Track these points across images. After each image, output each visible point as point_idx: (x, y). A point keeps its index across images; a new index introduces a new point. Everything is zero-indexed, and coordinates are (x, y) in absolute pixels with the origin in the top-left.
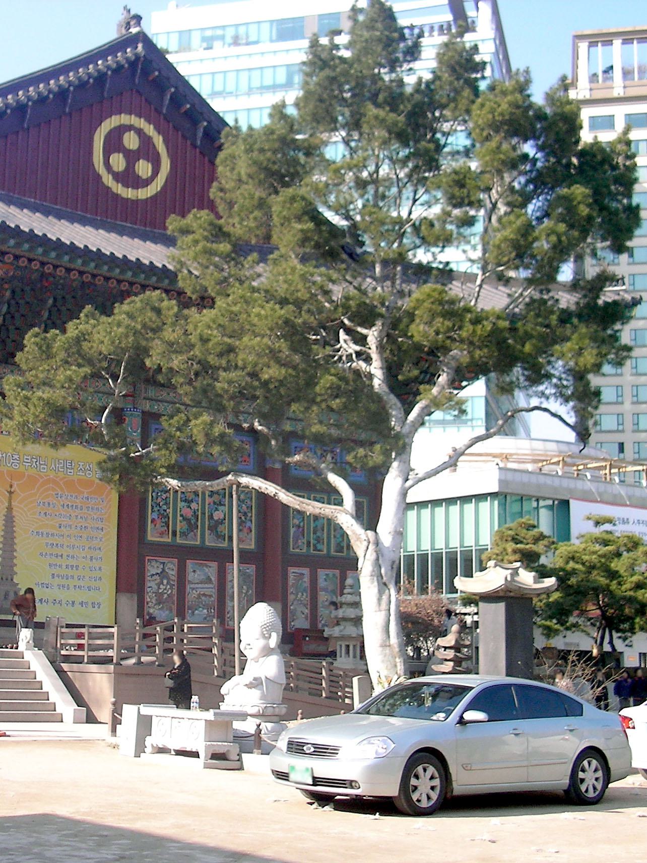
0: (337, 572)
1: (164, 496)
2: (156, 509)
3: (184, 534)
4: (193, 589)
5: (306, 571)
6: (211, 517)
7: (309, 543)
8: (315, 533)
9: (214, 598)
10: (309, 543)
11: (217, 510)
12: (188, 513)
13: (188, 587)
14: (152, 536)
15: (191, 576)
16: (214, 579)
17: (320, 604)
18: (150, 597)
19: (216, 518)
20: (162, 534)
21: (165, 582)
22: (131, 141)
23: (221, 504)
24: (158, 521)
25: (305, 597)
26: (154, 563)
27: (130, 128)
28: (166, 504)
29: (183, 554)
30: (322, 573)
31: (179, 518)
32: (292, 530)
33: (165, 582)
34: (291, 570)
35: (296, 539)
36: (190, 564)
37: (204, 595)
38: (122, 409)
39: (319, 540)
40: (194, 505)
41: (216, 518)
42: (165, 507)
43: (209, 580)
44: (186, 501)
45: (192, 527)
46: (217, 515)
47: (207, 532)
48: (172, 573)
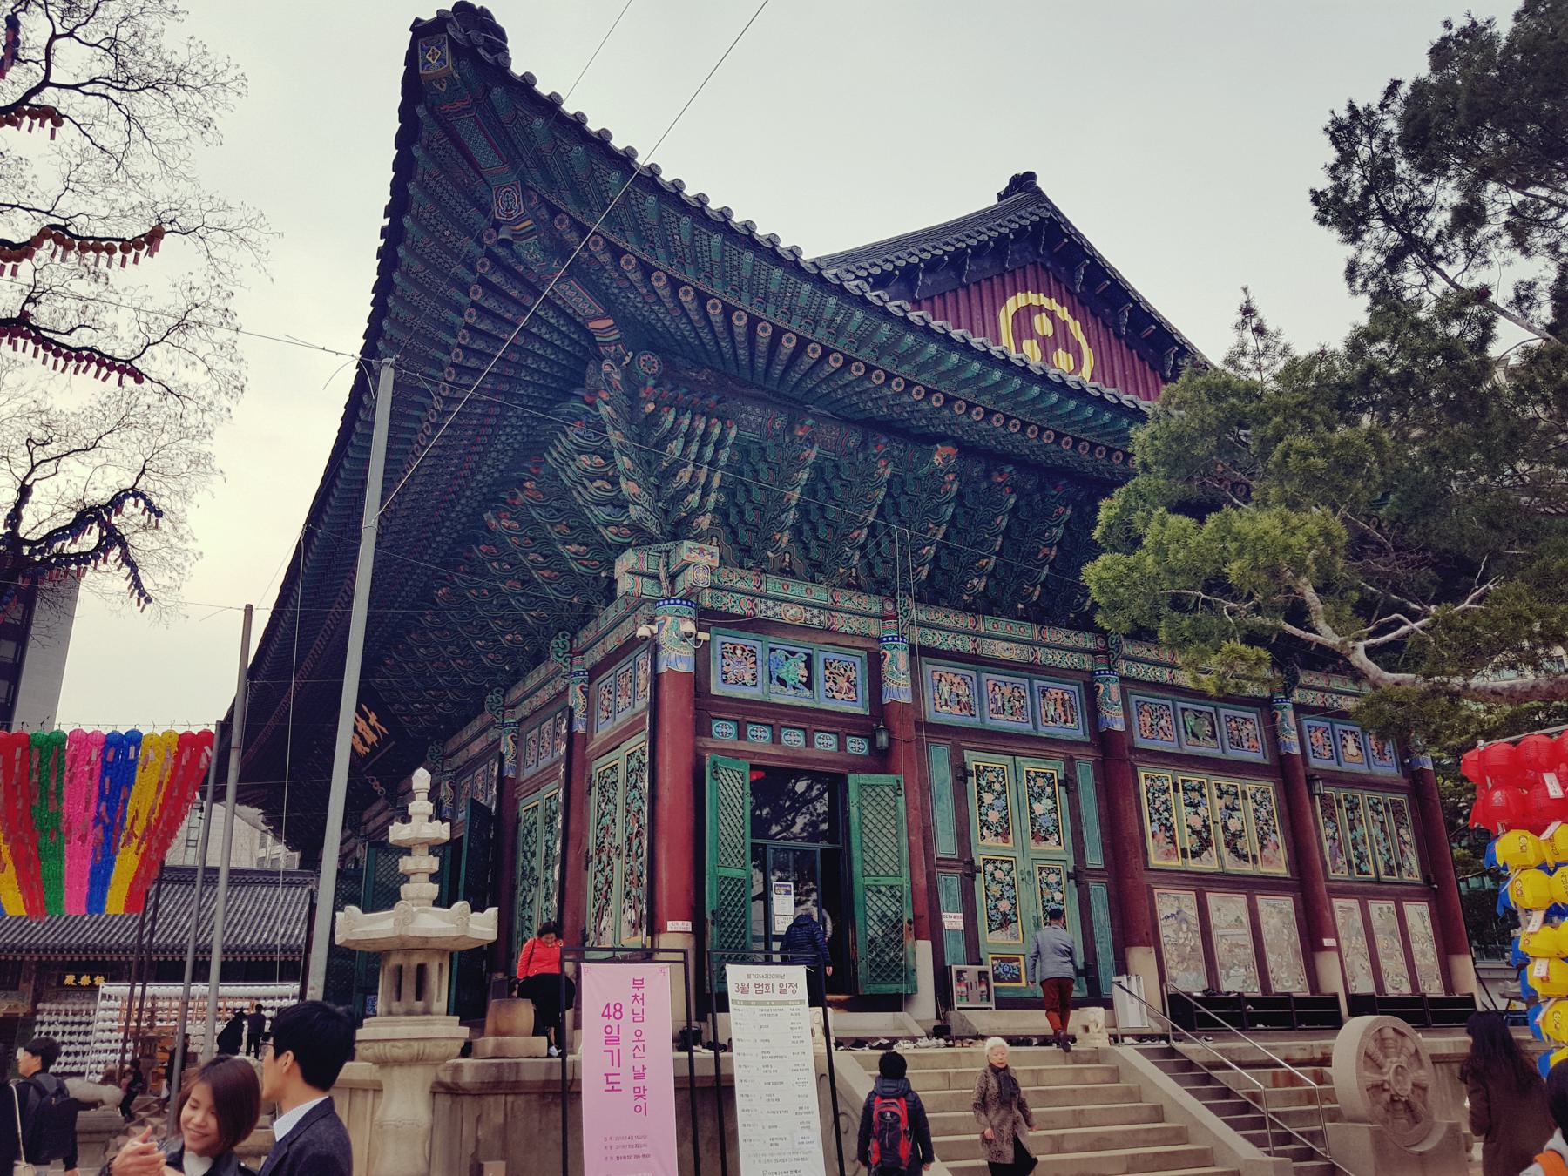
0: (1391, 904)
1: (1163, 798)
2: (1155, 817)
3: (1196, 854)
4: (1221, 936)
5: (1354, 904)
6: (1225, 828)
7: (1349, 863)
8: (1355, 848)
9: (1250, 950)
10: (1349, 863)
11: (1230, 817)
12: (1197, 823)
13: (1214, 933)
14: (1159, 858)
15: (1215, 918)
16: (1245, 919)
17: (1381, 955)
18: (1170, 954)
19: (1232, 829)
20: (1168, 854)
21: (1184, 927)
22: (1043, 325)
23: (1234, 809)
24: (1160, 835)
25: (1361, 942)
26: (1165, 898)
27: (1041, 309)
28: (1167, 809)
29: (1203, 883)
30: (1374, 906)
31: (1188, 831)
32: (1327, 845)
33: (1184, 927)
34: (1337, 903)
35: (1334, 858)
36: (1213, 899)
37: (1237, 945)
38: (1092, 673)
39: (1361, 857)
40: (1201, 810)
41: (1232, 829)
42: (1166, 814)
43: (1238, 919)
44: (1191, 805)
45: (1205, 844)
46: (1234, 825)
47: (1225, 851)
48: (1192, 913)
